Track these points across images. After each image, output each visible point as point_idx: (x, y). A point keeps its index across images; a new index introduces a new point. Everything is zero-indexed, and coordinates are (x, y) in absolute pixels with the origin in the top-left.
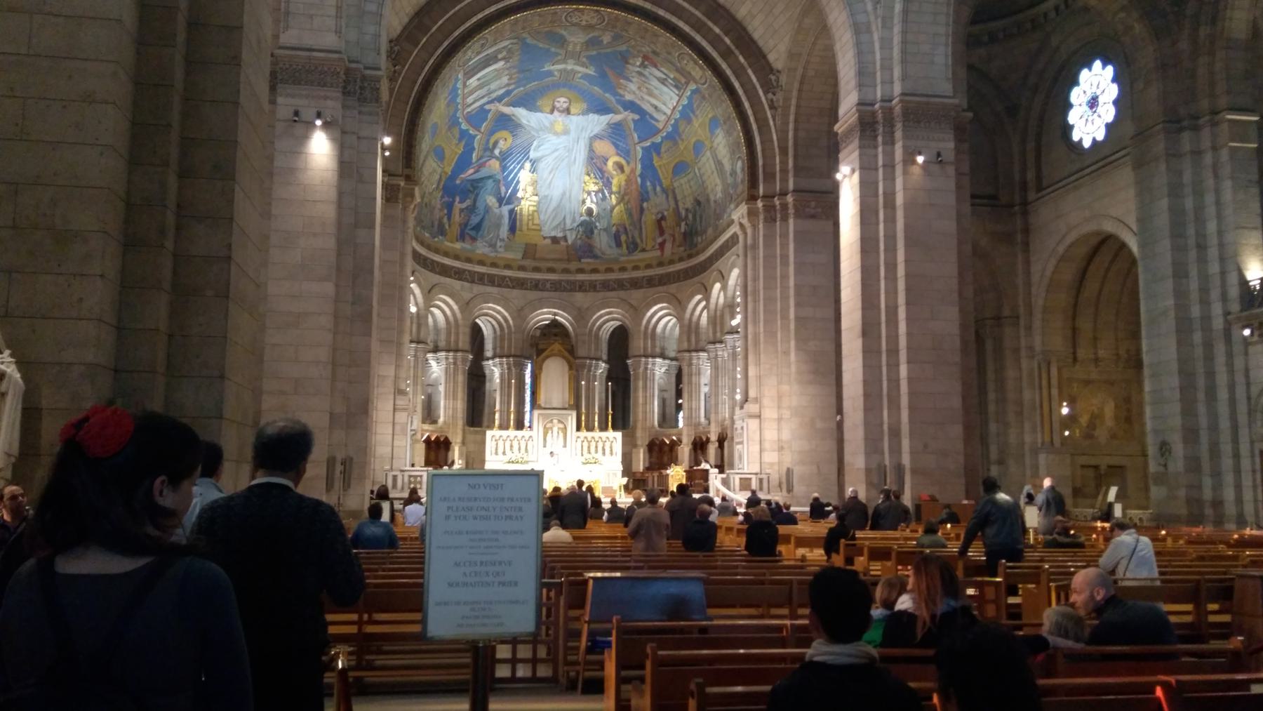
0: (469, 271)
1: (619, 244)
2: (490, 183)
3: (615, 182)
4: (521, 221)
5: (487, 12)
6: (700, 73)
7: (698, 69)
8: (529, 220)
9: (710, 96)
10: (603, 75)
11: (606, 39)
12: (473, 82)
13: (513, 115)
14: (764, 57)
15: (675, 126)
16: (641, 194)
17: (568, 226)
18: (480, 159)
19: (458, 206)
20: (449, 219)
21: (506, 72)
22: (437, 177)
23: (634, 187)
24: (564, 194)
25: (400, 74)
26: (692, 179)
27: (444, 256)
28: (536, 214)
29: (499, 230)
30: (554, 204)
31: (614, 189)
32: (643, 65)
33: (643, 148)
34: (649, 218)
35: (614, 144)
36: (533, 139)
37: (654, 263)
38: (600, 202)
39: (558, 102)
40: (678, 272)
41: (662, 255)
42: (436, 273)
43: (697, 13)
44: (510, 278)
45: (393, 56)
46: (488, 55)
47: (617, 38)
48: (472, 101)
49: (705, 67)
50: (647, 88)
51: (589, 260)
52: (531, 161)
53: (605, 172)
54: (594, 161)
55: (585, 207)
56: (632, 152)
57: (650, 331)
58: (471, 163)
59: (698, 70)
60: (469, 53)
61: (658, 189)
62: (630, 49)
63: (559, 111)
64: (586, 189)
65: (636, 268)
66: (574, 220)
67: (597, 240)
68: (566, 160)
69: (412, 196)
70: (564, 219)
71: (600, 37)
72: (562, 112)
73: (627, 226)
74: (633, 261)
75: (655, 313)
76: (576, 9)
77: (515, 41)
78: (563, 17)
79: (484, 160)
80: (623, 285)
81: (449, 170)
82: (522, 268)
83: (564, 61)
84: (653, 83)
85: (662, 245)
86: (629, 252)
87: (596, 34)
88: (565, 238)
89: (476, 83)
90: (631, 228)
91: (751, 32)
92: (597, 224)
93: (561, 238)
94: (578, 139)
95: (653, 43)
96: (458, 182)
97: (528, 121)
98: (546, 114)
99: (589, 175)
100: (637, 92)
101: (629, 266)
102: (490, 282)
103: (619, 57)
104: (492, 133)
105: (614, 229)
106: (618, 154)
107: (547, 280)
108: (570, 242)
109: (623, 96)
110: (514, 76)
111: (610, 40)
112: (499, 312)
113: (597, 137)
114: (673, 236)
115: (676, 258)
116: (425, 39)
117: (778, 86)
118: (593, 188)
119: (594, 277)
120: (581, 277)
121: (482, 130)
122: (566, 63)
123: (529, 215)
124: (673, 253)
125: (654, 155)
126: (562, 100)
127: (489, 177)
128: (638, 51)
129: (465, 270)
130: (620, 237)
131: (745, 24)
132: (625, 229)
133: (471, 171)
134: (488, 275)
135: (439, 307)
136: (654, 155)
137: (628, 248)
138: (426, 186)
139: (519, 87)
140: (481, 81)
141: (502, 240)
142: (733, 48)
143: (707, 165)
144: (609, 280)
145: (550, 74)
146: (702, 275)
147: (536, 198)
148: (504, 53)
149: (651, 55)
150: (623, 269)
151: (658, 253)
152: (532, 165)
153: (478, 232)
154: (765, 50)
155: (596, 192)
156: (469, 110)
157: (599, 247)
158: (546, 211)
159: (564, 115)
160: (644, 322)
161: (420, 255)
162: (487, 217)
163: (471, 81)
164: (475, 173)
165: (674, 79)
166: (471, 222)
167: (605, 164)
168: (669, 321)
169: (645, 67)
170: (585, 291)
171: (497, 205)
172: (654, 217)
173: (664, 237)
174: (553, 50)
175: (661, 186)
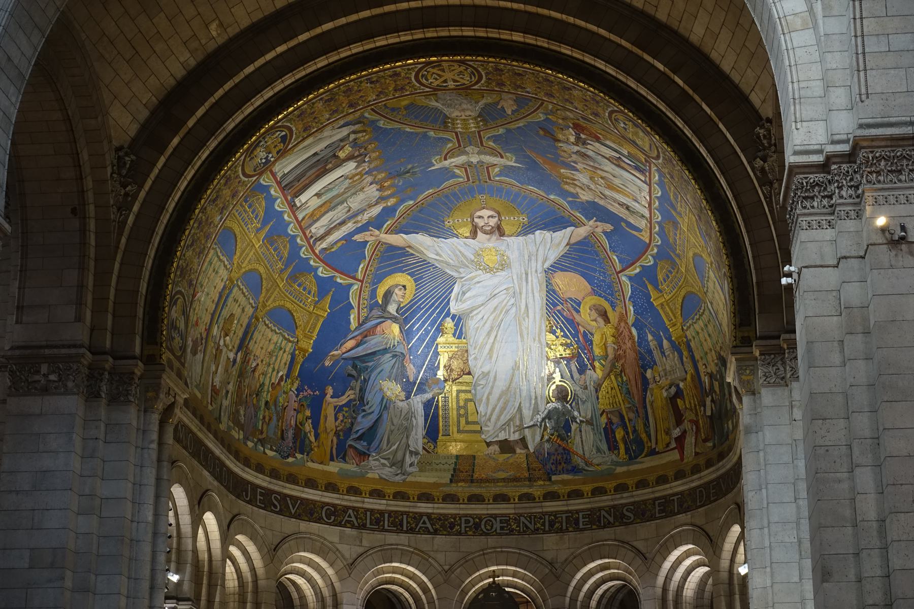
0: (354, 509)
1: (613, 446)
2: (387, 361)
3: (596, 339)
4: (446, 418)
5: (279, 86)
6: (647, 139)
7: (641, 134)
8: (459, 416)
9: (672, 177)
10: (533, 166)
11: (509, 105)
12: (308, 198)
13: (410, 247)
14: (745, 99)
15: (662, 233)
16: (640, 357)
17: (528, 422)
18: (364, 322)
19: (331, 402)
20: (316, 426)
21: (369, 179)
22: (287, 358)
23: (629, 344)
24: (516, 367)
25: (135, 197)
26: (709, 321)
27: (306, 486)
28: (471, 406)
29: (408, 437)
30: (501, 385)
31: (597, 351)
32: (578, 138)
33: (630, 278)
34: (658, 395)
35: (584, 275)
36: (450, 282)
37: (671, 473)
38: (576, 375)
39: (480, 217)
40: (706, 486)
41: (682, 459)
42: (291, 516)
43: (624, 43)
44: (429, 515)
45: (124, 172)
46: (315, 154)
47: (521, 102)
48: (322, 231)
49: (648, 129)
50: (602, 178)
51: (566, 477)
52: (453, 319)
53: (578, 324)
54: (559, 308)
55: (554, 387)
56: (617, 287)
57: (671, 596)
58: (349, 331)
59: (647, 140)
60: (261, 154)
61: (665, 343)
62: (550, 117)
63: (485, 233)
64: (551, 355)
65: (642, 484)
66: (536, 411)
67: (578, 439)
68: (514, 309)
69: (157, 388)
70: (520, 409)
71: (498, 103)
72: (490, 233)
73: (624, 413)
74: (635, 473)
75: (679, 562)
76: (428, 64)
77: (357, 127)
78: (413, 79)
79: (369, 324)
80: (623, 516)
81: (308, 345)
82: (450, 498)
83: (459, 150)
84: (606, 169)
85: (680, 440)
86: (631, 458)
87: (488, 100)
88: (523, 440)
89: (316, 203)
90: (632, 415)
91: (718, 62)
92: (576, 413)
93: (516, 442)
94: (527, 274)
95: (567, 100)
96: (327, 363)
97: (438, 254)
98: (461, 241)
99: (554, 332)
100: (592, 187)
101: (631, 482)
102: (393, 524)
103: (541, 132)
104: (379, 279)
105: (604, 420)
106: (595, 293)
107: (495, 516)
108: (532, 450)
109: (576, 196)
110: (386, 184)
111: (515, 107)
112: (412, 577)
113: (558, 266)
114: (696, 423)
115: (702, 461)
116: (176, 141)
117: (770, 145)
118: (561, 351)
119: (576, 504)
120: (551, 506)
121: (360, 276)
122: (466, 153)
123: (459, 408)
124: (697, 454)
125: (650, 287)
126: (486, 213)
127: (385, 351)
128: (563, 119)
129: (348, 508)
130: (613, 432)
131: (706, 50)
132: (622, 417)
133: (350, 344)
134: (390, 513)
135: (302, 574)
136: (650, 287)
137: (627, 450)
138: (264, 374)
139: (402, 201)
140: (324, 198)
141: (417, 453)
142: (691, 92)
143: (716, 294)
144: (600, 509)
145: (447, 173)
146: (735, 490)
147: (466, 378)
148: (348, 150)
149: (582, 122)
150: (621, 488)
151: (675, 455)
152: (457, 325)
153: (369, 444)
154: (745, 88)
155: (569, 360)
156: (324, 245)
157: (581, 452)
158: (488, 399)
159: (494, 238)
160: (661, 580)
161: (255, 487)
162: (385, 416)
163: (303, 198)
164: (357, 345)
165: (630, 156)
166: (356, 428)
167: (578, 312)
168: (706, 576)
169: (584, 143)
170: (561, 530)
171: (403, 395)
172: (665, 394)
173: (682, 427)
174: (432, 133)
175: (669, 339)
